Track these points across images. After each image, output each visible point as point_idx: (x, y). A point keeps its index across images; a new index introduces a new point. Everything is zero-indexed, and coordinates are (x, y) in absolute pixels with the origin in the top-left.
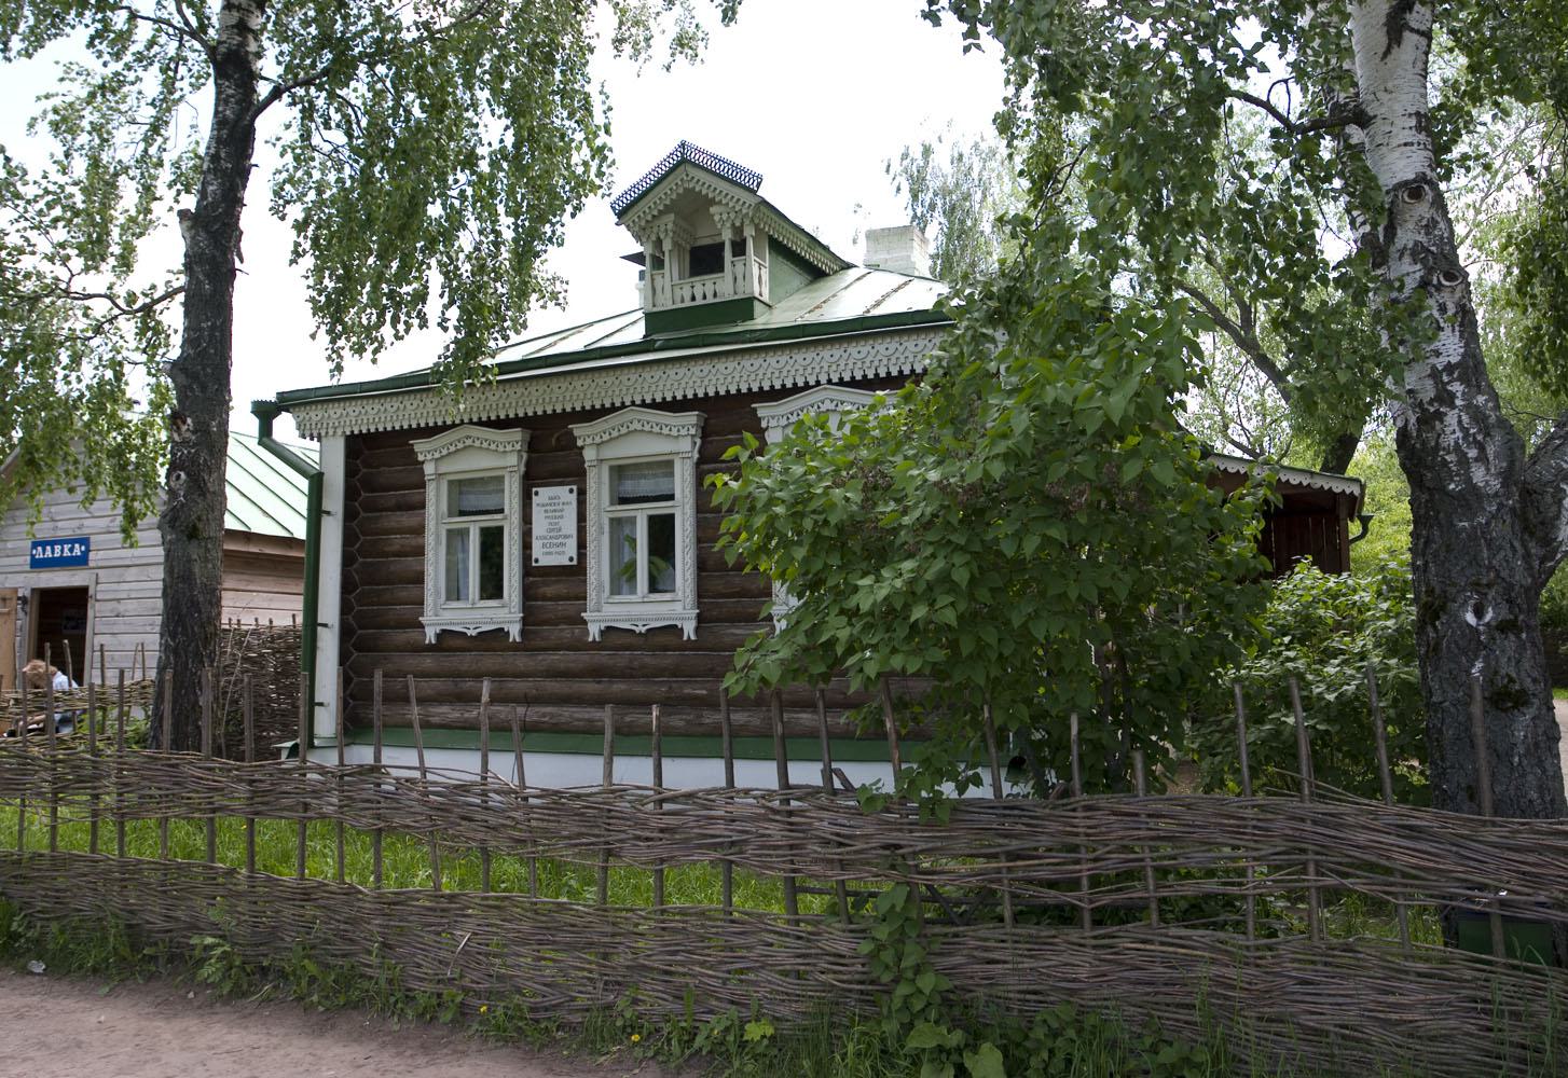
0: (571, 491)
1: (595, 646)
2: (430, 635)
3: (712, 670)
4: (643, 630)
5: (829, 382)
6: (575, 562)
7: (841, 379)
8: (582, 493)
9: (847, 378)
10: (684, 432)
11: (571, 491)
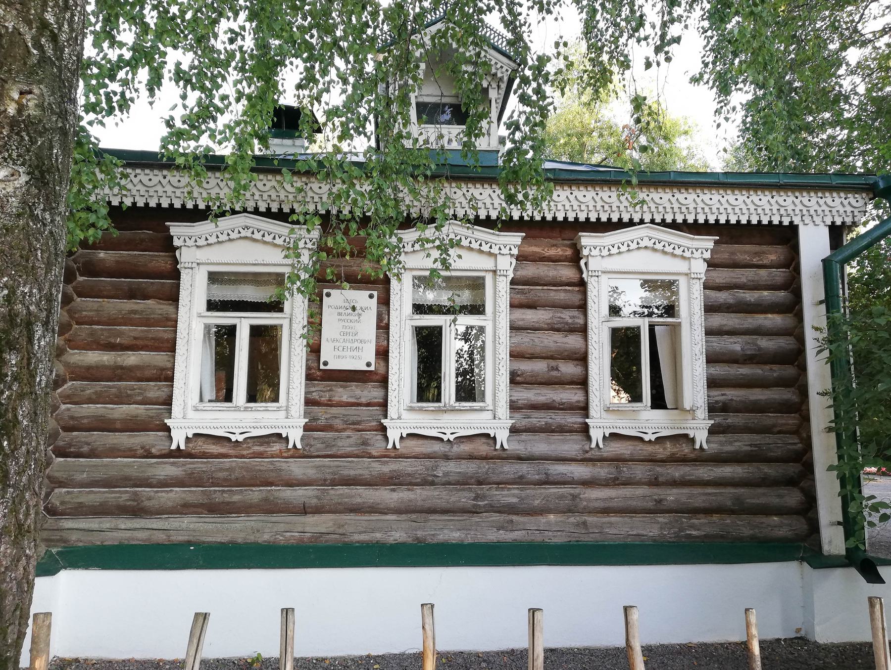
0: (371, 296)
1: (396, 455)
2: (179, 439)
3: (521, 477)
4: (452, 438)
5: (652, 221)
6: (372, 368)
7: (663, 220)
8: (385, 301)
9: (669, 220)
10: (505, 251)
11: (371, 296)
